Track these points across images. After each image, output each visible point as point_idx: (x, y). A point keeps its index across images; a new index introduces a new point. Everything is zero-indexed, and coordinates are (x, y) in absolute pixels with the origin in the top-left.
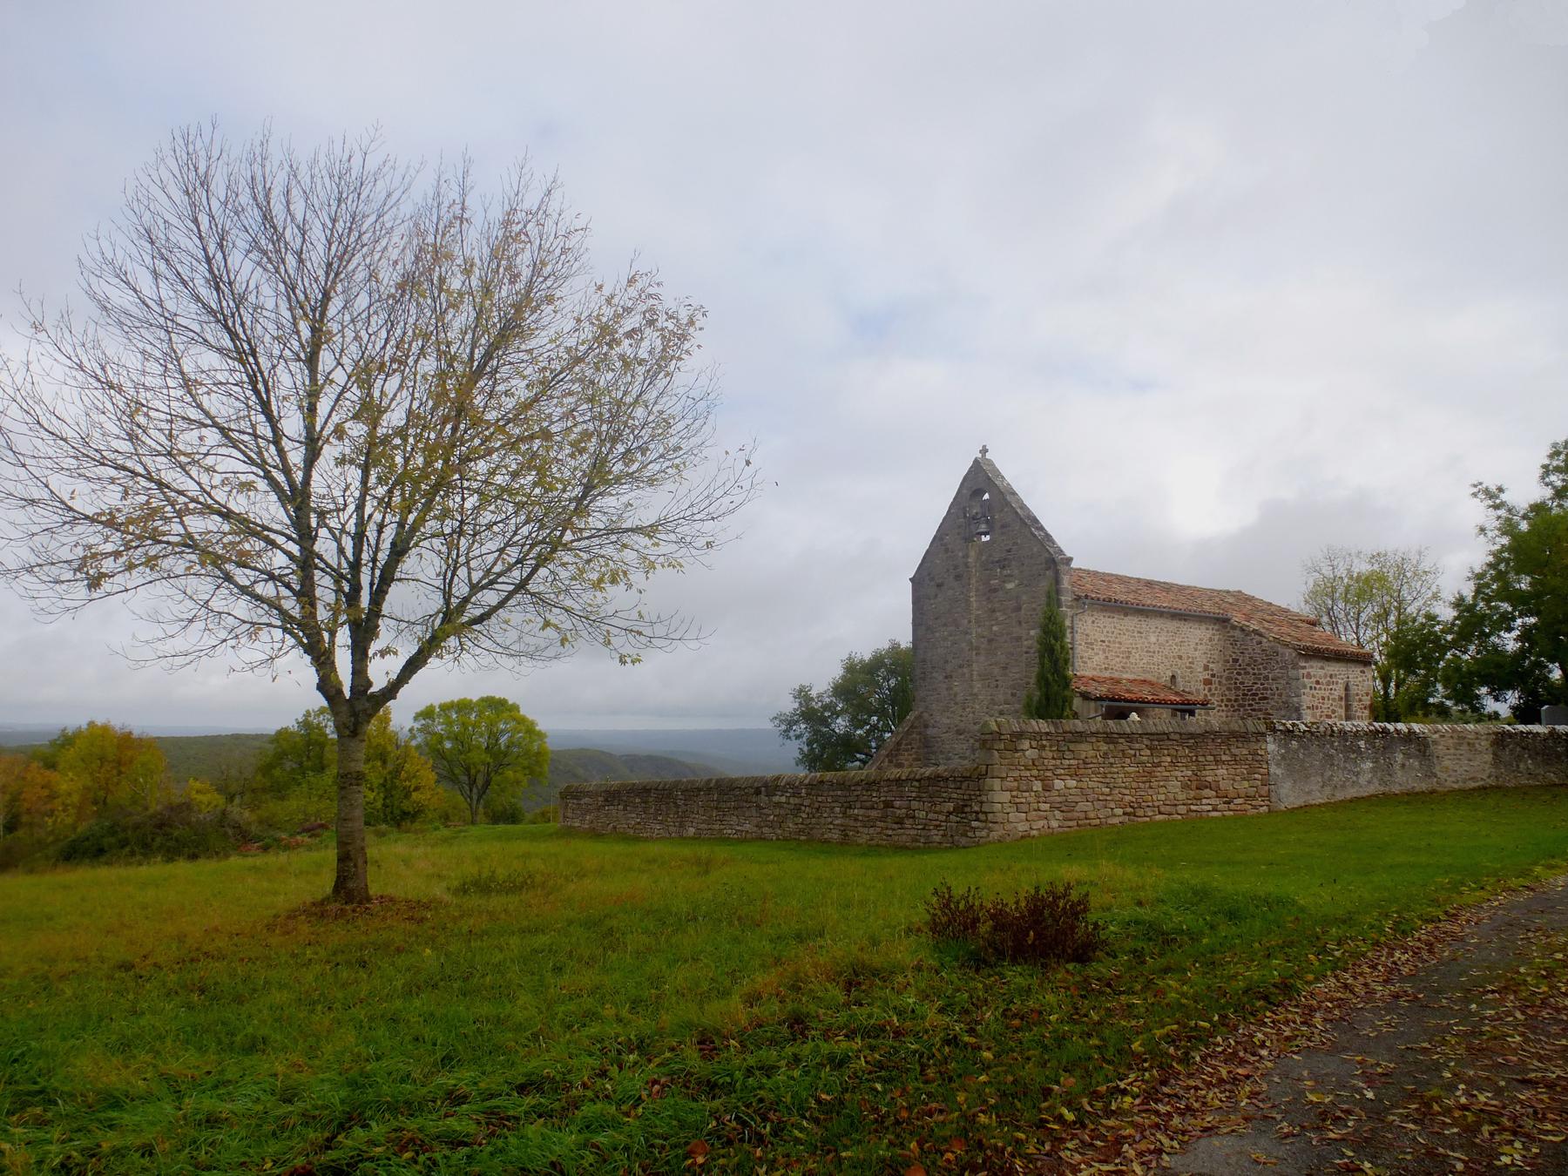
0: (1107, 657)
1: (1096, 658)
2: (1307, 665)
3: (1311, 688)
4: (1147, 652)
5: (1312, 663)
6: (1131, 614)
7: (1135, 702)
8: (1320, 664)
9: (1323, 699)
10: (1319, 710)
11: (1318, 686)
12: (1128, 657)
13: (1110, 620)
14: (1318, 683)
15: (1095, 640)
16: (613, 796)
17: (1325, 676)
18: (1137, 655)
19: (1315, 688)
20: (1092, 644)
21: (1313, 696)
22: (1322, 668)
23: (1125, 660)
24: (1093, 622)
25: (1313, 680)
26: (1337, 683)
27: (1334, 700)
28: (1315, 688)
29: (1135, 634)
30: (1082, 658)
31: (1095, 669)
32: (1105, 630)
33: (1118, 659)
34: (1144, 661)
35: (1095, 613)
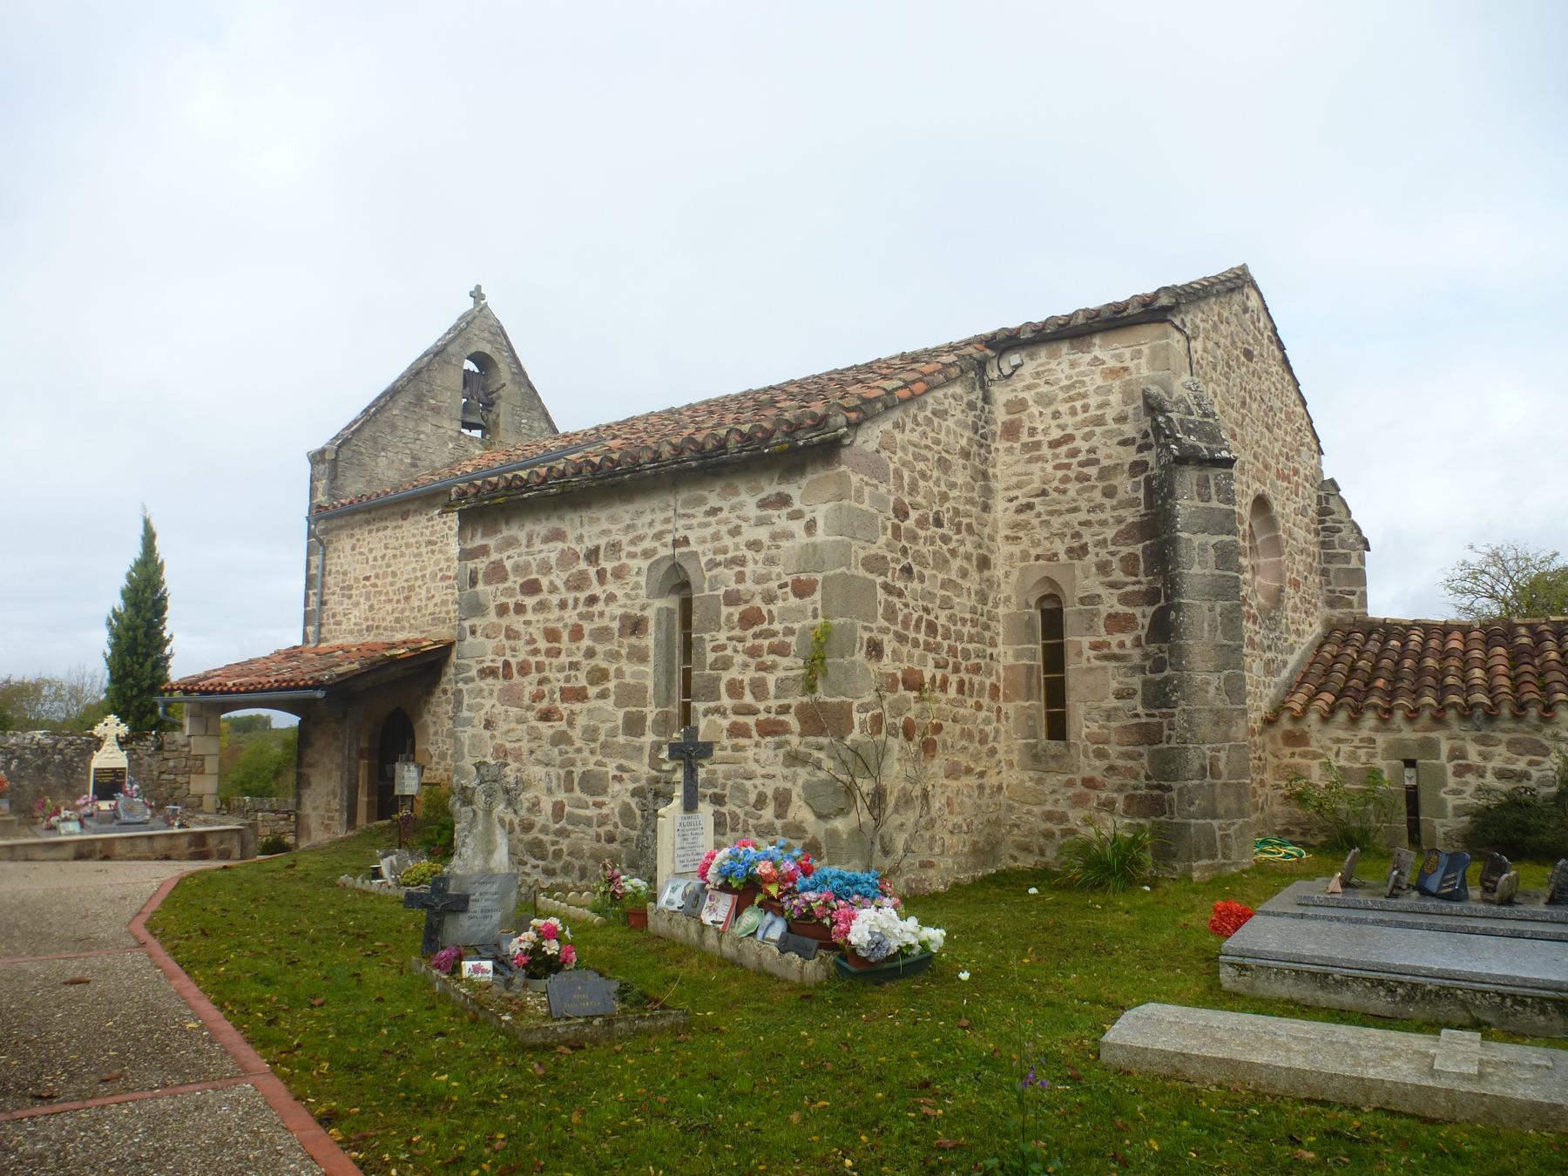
0: (371, 607)
1: (356, 612)
2: (491, 542)
3: (502, 610)
4: (442, 579)
5: (507, 532)
6: (417, 512)
7: (214, 692)
8: (542, 528)
9: (553, 635)
10: (534, 676)
11: (530, 601)
12: (407, 599)
13: (381, 534)
14: (531, 588)
15: (356, 579)
16: (1524, 1036)
17: (567, 559)
18: (423, 592)
19: (520, 609)
20: (350, 588)
21: (511, 634)
22: (558, 535)
23: (400, 606)
24: (353, 548)
25: (515, 581)
26: (619, 574)
27: (602, 634)
28: (520, 609)
29: (423, 550)
30: (334, 615)
31: (351, 632)
32: (371, 558)
33: (389, 607)
34: (437, 600)
35: (357, 531)
